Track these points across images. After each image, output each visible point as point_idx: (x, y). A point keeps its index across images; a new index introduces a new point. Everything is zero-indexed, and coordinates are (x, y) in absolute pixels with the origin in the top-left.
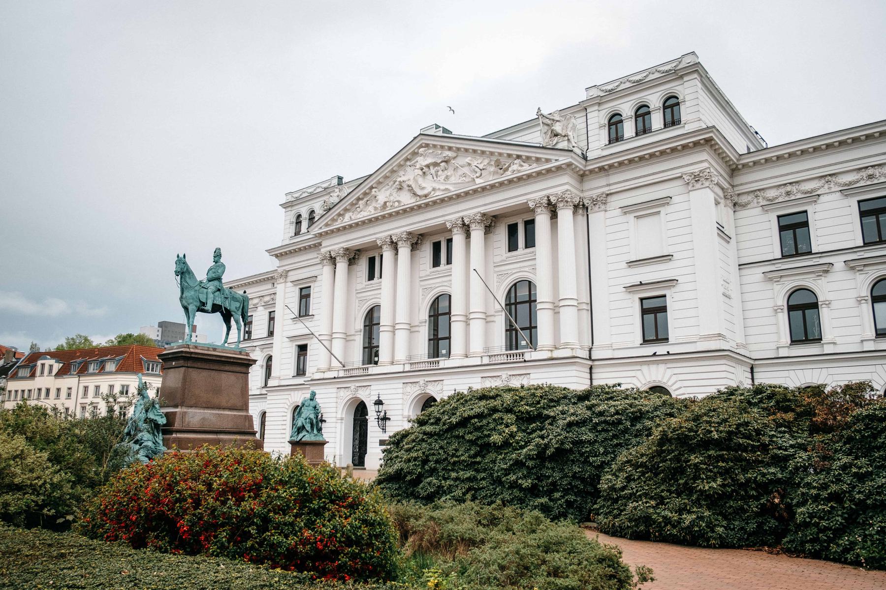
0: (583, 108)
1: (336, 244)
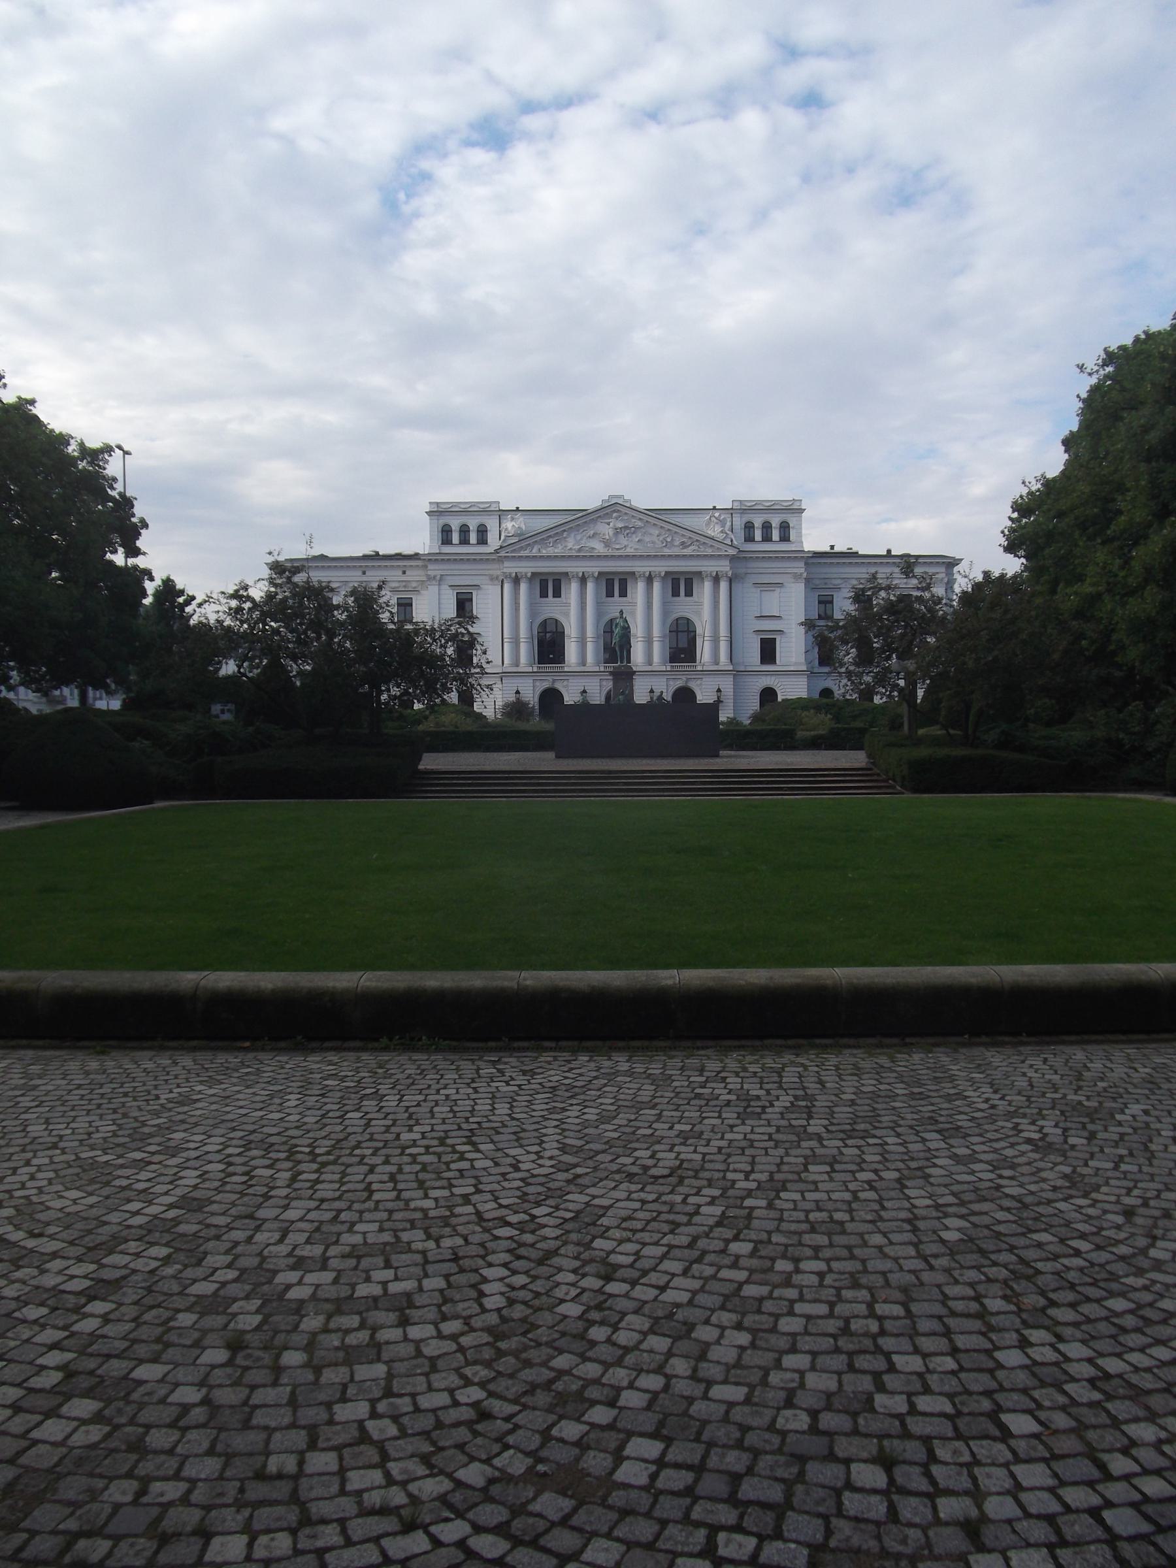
0: (731, 511)
1: (527, 568)
